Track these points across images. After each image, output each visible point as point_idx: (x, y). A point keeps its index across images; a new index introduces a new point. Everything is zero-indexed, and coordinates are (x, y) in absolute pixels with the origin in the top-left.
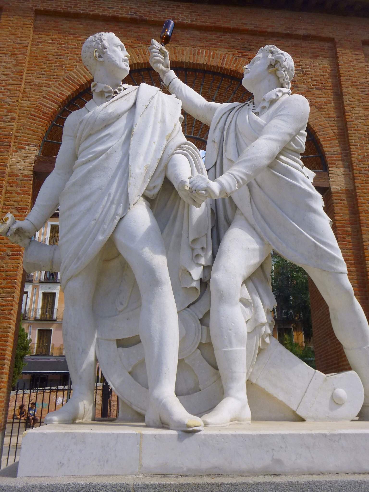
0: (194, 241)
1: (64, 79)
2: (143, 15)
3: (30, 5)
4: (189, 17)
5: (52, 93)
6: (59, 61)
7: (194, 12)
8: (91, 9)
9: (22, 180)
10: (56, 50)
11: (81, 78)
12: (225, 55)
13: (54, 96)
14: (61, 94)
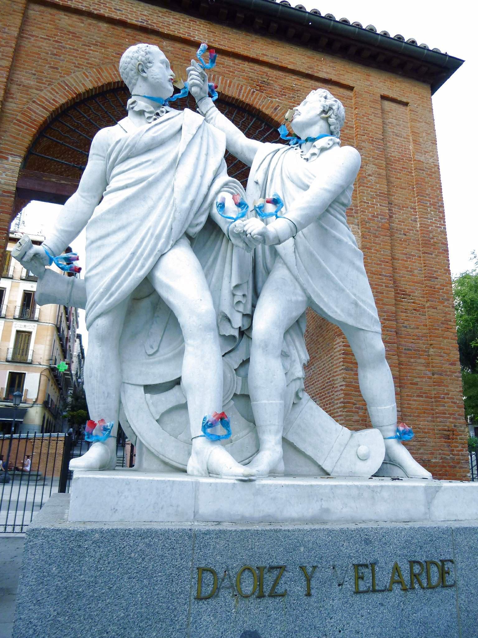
0: (237, 287)
1: (59, 84)
2: (155, 25)
4: (206, 36)
5: (44, 98)
6: (53, 61)
7: (211, 32)
8: (96, 8)
10: (51, 48)
11: (79, 85)
12: (242, 86)
13: (46, 103)
14: (54, 100)
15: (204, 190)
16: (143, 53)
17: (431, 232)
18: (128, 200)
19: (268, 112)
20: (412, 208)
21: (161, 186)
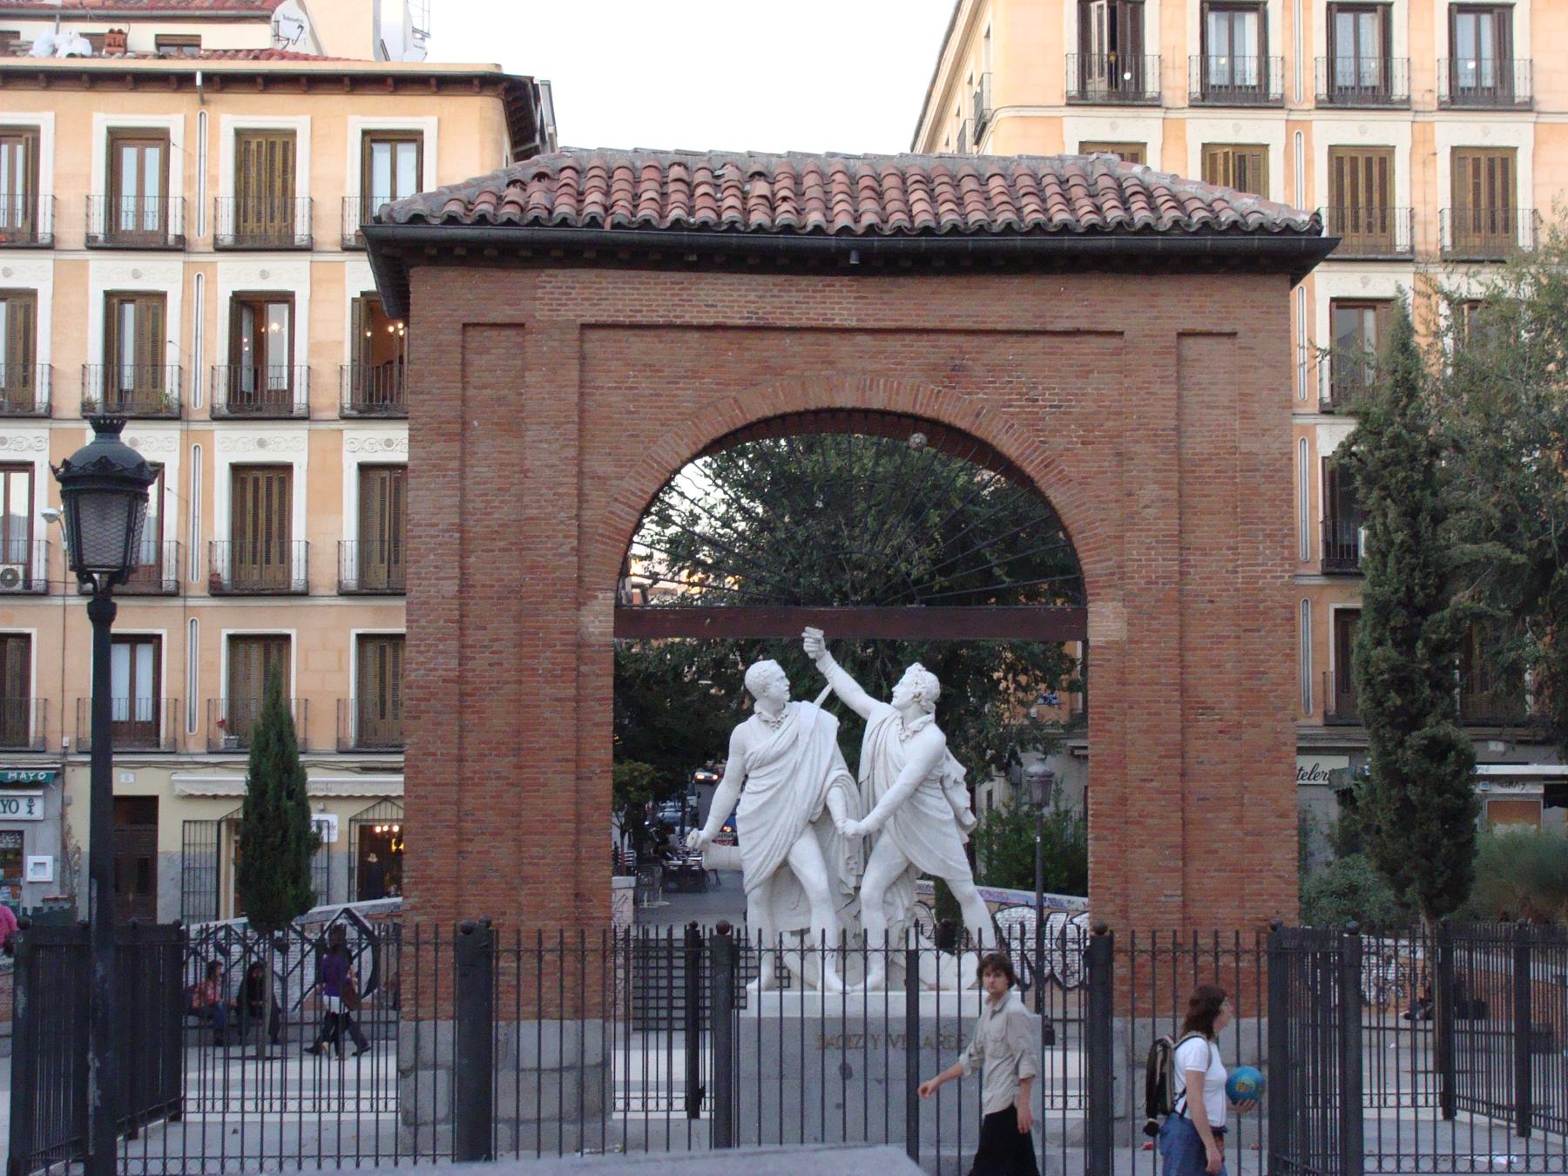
3: (571, 315)
17: (1261, 589)
18: (764, 804)
19: (963, 424)
20: (1229, 548)
21: (786, 792)
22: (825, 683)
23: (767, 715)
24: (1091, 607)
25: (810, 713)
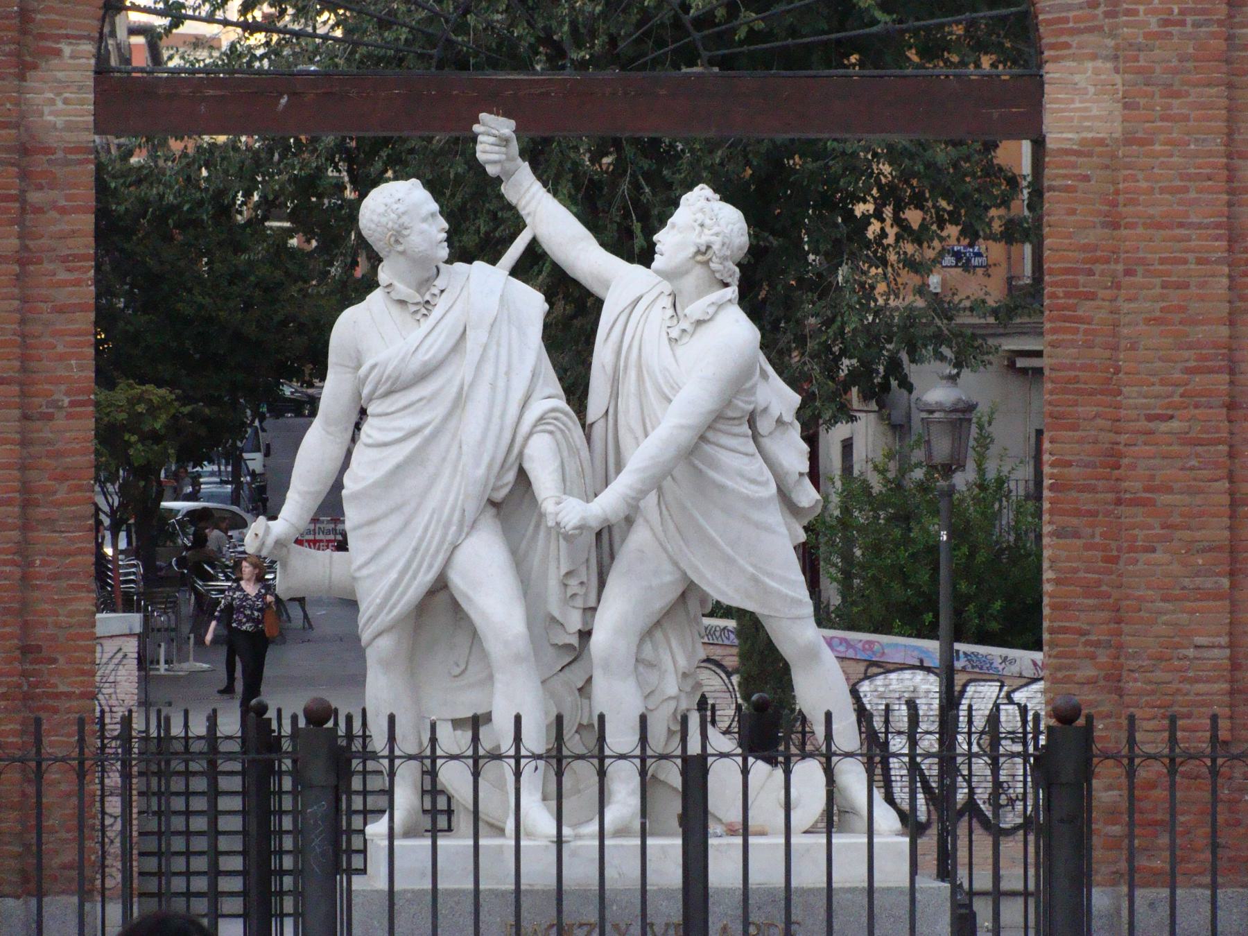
0: (569, 574)
9: (67, 163)
15: (507, 436)
16: (393, 216)
18: (399, 468)
21: (444, 440)
22: (519, 224)
23: (403, 290)
24: (1052, 72)
25: (488, 286)
